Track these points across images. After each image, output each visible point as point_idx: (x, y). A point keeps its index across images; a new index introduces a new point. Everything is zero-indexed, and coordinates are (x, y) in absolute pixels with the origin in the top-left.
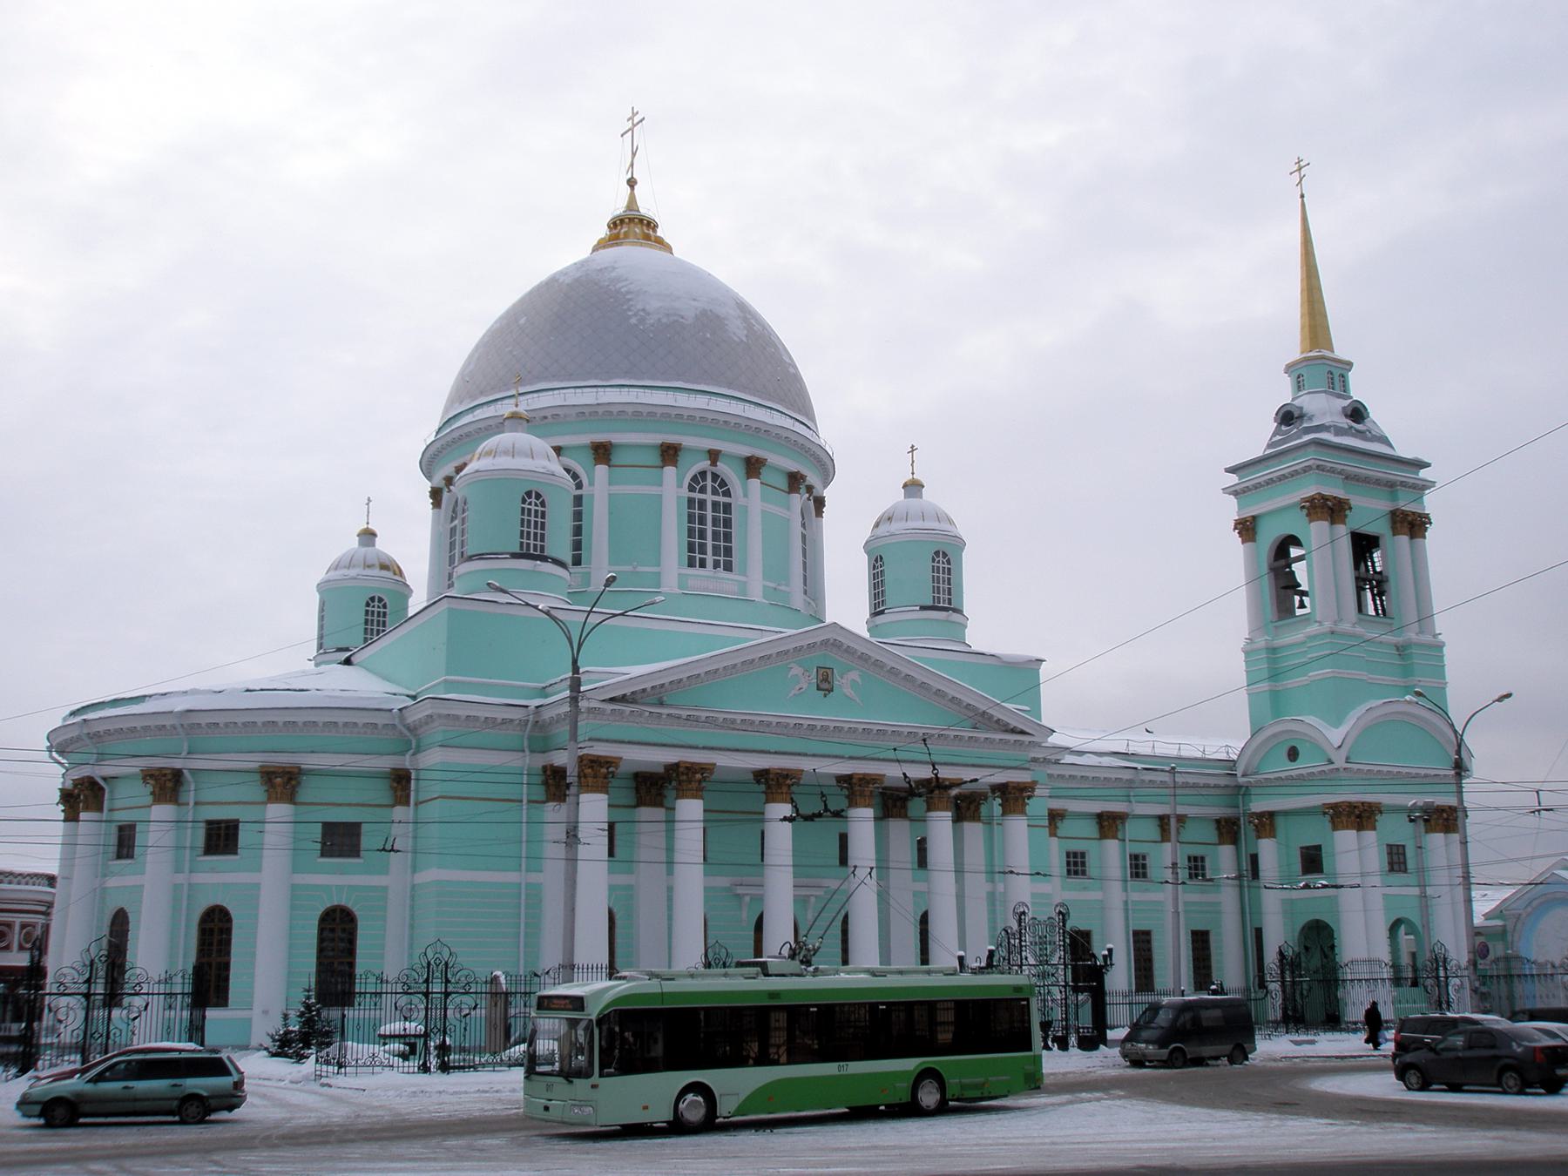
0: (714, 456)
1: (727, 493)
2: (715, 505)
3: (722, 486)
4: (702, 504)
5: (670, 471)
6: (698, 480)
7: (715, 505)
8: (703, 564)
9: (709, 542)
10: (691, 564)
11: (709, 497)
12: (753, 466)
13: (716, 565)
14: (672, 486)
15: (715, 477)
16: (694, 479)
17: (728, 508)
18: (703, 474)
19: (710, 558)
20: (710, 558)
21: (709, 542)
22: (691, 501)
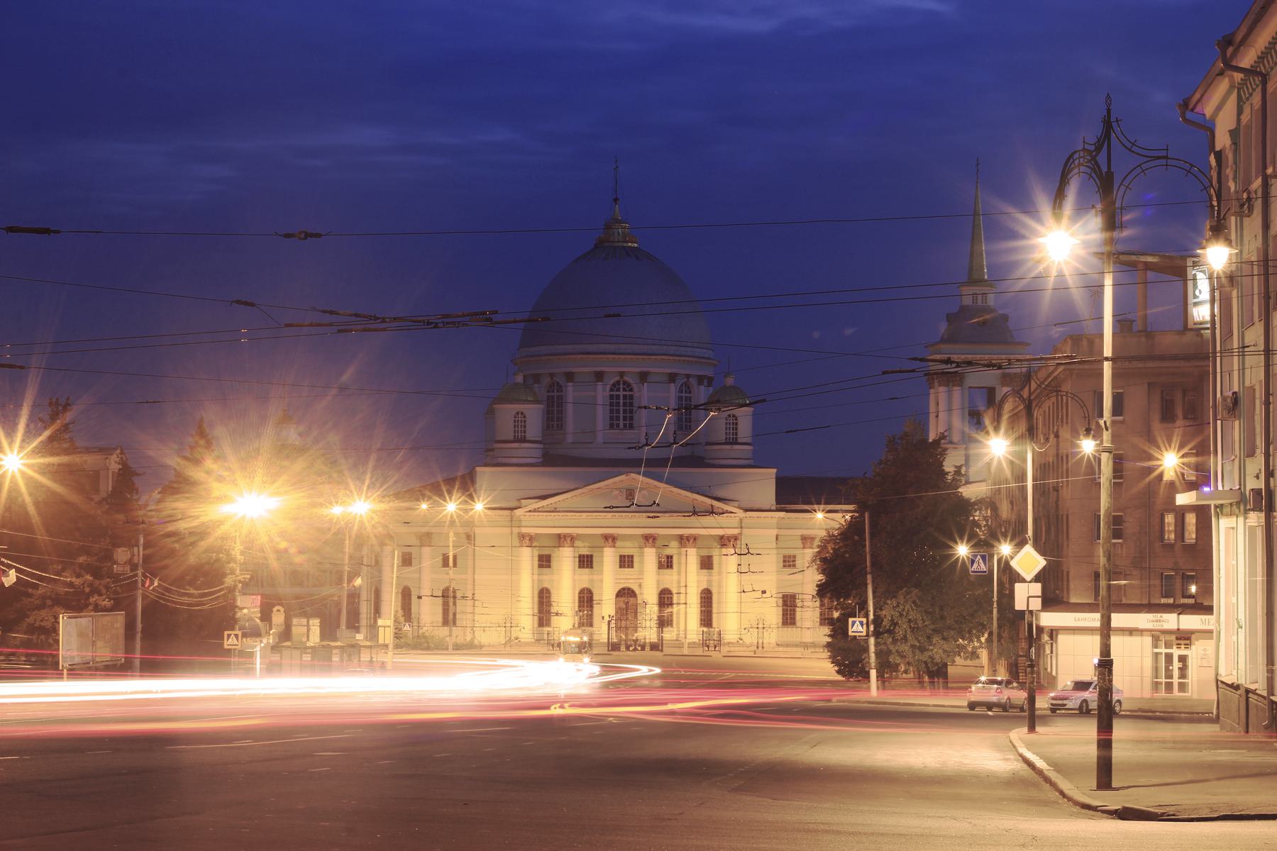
0: (622, 374)
1: (631, 390)
2: (625, 396)
3: (628, 386)
4: (618, 396)
5: (600, 386)
6: (615, 386)
7: (625, 396)
8: (618, 425)
9: (621, 415)
10: (612, 426)
11: (621, 393)
12: (643, 377)
13: (625, 425)
14: (602, 393)
15: (625, 383)
16: (614, 385)
17: (631, 397)
18: (618, 382)
19: (621, 423)
20: (621, 423)
21: (621, 415)
22: (612, 397)
